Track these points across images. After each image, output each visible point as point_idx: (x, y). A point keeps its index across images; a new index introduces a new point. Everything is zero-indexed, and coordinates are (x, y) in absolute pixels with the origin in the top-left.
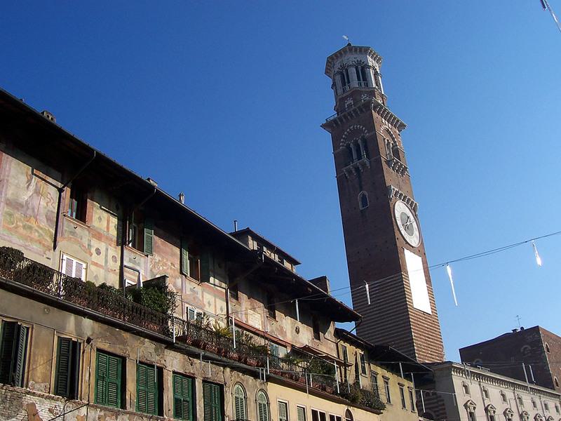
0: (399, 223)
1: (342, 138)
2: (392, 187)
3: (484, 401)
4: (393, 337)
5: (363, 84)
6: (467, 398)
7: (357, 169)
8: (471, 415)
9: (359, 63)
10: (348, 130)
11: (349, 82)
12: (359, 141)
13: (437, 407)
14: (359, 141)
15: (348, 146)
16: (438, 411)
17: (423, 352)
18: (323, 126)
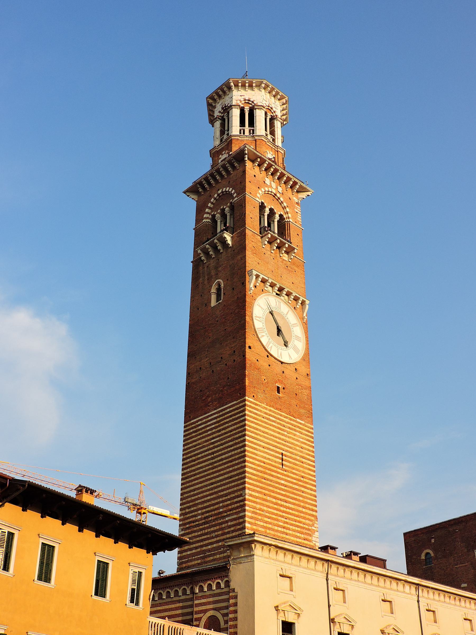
0: (258, 324)
1: (207, 207)
2: (255, 273)
3: (329, 606)
4: (222, 496)
5: (247, 133)
6: (283, 598)
7: (215, 247)
8: (288, 627)
9: (248, 102)
10: (216, 196)
11: (228, 130)
12: (227, 209)
13: (227, 607)
14: (227, 209)
15: (214, 216)
16: (227, 615)
17: (266, 522)
18: (185, 192)
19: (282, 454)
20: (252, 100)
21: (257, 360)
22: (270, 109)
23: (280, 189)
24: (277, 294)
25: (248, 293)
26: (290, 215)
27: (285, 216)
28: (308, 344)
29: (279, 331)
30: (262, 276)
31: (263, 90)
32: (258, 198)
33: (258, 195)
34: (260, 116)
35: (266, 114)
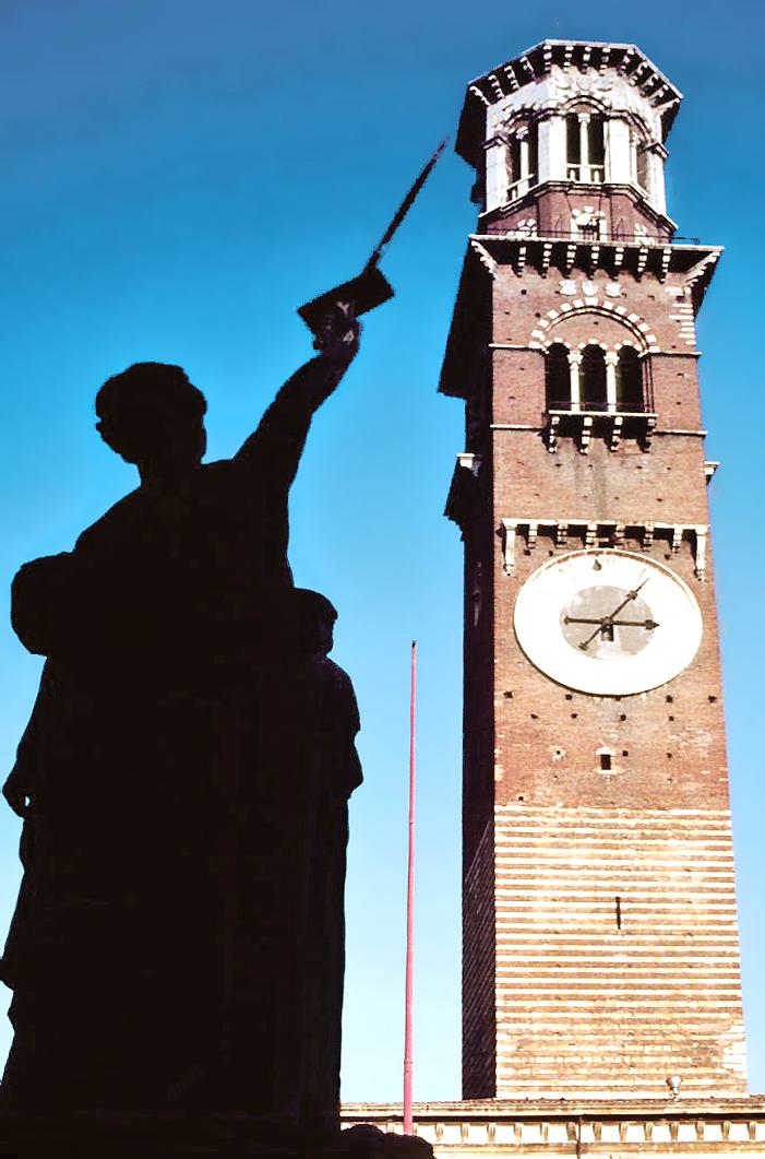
2: (511, 523)
19: (618, 900)
20: (528, 106)
21: (534, 717)
22: (585, 100)
23: (614, 288)
24: (602, 545)
25: (501, 576)
26: (651, 338)
27: (638, 347)
28: (716, 626)
29: (607, 627)
30: (534, 525)
31: (555, 69)
32: (537, 340)
33: (536, 333)
34: (554, 135)
35: (573, 122)
